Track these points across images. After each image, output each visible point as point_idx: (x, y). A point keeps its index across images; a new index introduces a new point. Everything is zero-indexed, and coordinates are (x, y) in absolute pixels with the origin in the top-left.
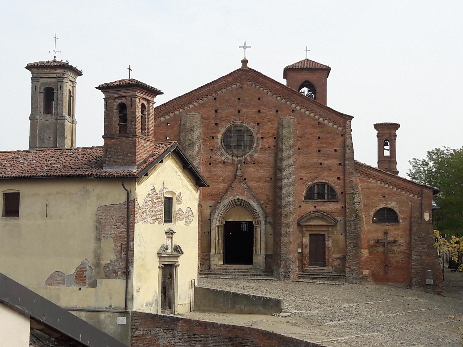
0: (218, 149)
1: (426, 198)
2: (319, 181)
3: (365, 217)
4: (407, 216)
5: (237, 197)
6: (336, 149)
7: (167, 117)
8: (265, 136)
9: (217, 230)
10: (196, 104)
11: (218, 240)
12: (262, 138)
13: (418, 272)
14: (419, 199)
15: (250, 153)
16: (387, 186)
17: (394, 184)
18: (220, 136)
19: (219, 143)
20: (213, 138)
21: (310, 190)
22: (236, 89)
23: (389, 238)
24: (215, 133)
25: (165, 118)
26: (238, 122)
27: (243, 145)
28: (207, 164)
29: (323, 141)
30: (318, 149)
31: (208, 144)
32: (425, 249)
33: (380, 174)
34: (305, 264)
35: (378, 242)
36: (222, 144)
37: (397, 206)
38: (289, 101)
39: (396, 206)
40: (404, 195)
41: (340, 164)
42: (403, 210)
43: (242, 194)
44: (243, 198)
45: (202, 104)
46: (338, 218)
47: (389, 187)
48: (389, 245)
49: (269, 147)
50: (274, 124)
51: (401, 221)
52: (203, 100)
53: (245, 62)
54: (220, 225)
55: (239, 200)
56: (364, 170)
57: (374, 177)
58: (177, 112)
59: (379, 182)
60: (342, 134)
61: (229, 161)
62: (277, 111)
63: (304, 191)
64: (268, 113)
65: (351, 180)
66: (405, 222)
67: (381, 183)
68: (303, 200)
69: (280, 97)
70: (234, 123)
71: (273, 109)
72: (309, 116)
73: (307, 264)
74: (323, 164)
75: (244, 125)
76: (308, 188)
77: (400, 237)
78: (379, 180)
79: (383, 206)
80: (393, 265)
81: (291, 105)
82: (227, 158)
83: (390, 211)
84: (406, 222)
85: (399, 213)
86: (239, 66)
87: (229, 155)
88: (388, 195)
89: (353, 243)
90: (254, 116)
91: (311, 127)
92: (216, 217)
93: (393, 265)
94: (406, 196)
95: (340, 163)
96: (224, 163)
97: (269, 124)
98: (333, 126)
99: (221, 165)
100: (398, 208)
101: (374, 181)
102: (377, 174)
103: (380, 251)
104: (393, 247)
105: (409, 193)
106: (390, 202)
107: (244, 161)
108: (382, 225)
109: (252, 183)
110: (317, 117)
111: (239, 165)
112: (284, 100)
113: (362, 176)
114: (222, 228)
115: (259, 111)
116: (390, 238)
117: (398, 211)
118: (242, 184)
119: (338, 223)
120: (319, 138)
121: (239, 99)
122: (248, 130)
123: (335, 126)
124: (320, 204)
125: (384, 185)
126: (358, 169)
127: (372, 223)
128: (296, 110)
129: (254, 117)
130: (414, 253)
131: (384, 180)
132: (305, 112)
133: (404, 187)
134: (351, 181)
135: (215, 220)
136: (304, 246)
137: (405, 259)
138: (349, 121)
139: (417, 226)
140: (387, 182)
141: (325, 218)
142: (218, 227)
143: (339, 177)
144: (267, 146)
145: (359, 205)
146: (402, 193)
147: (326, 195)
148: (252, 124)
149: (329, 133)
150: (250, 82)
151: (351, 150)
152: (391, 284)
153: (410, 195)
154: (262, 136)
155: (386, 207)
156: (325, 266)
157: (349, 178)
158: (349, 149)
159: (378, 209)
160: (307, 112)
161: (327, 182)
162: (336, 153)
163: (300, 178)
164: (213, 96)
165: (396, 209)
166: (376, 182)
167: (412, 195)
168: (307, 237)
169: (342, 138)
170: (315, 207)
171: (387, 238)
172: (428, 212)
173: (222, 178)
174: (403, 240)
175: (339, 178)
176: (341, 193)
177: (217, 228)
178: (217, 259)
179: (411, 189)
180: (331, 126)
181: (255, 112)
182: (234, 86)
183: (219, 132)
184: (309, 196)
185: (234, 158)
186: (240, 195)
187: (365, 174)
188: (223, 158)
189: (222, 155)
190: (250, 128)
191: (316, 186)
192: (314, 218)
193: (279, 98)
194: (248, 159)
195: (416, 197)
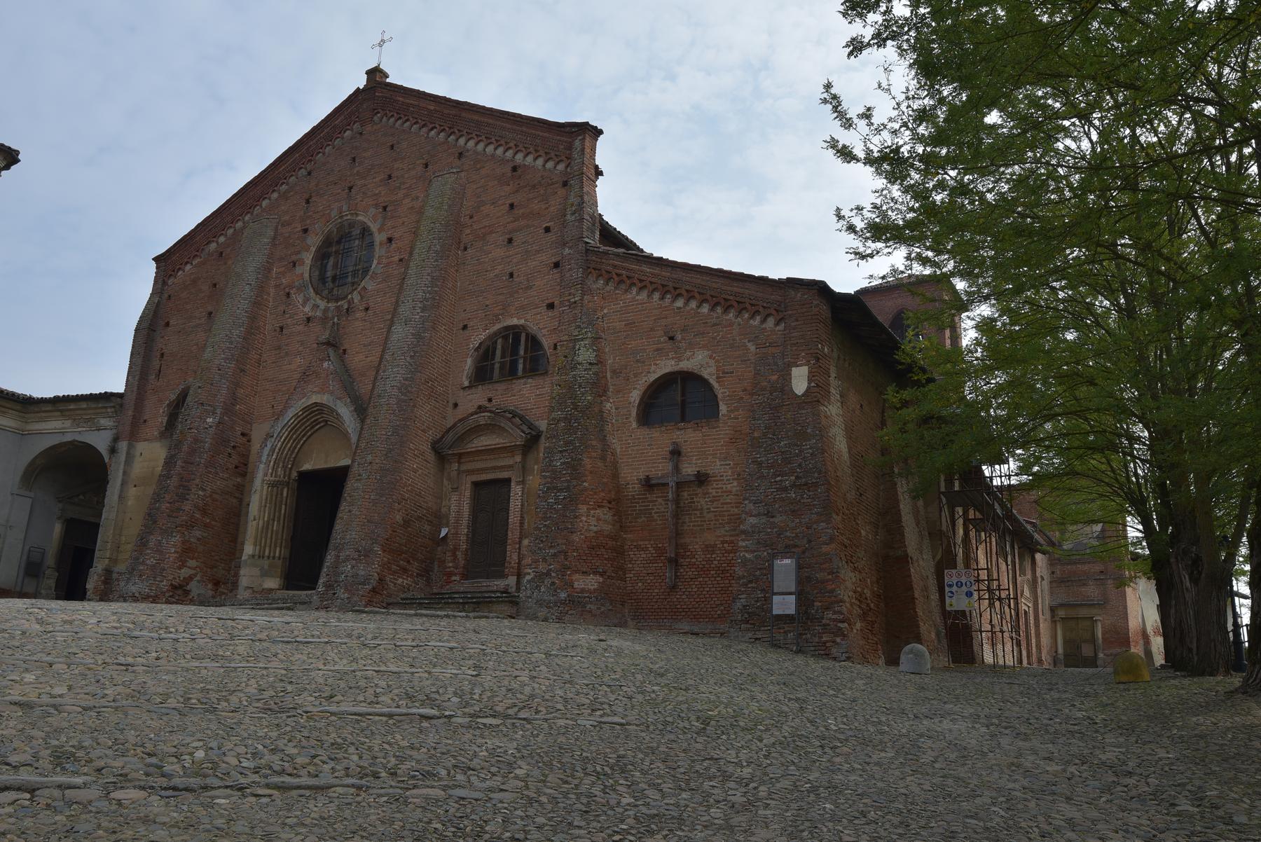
0: (301, 289)
1: (797, 320)
2: (505, 324)
3: (616, 409)
4: (745, 390)
5: (315, 398)
6: (547, 225)
7: (222, 239)
8: (396, 235)
9: (265, 493)
10: (275, 195)
11: (266, 519)
12: (390, 240)
13: (758, 573)
14: (778, 328)
15: (363, 284)
16: (680, 303)
17: (699, 293)
18: (308, 258)
19: (306, 275)
20: (294, 265)
21: (485, 354)
22: (351, 139)
23: (684, 470)
24: (299, 252)
25: (217, 242)
26: (346, 215)
27: (351, 269)
28: (275, 330)
29: (521, 211)
30: (507, 236)
31: (284, 281)
32: (785, 489)
33: (657, 271)
34: (450, 574)
35: (649, 484)
36: (310, 276)
37: (712, 362)
38: (454, 132)
39: (707, 363)
40: (731, 325)
41: (557, 265)
42: (733, 373)
43: (322, 391)
44: (324, 399)
45: (285, 193)
46: (543, 425)
47: (686, 304)
48: (685, 494)
49: (401, 260)
50: (417, 198)
51: (723, 408)
52: (287, 184)
53: (375, 74)
54: (277, 479)
55: (318, 409)
56: (615, 266)
57: (641, 281)
58: (240, 224)
59: (656, 296)
60: (565, 179)
61: (319, 314)
62: (426, 166)
63: (469, 361)
64: (406, 176)
65: (573, 300)
66: (737, 409)
67: (662, 298)
68: (466, 383)
69: (435, 130)
70: (339, 220)
71: (418, 162)
72: (493, 156)
73: (455, 575)
74: (515, 275)
75: (360, 218)
76: (481, 351)
77: (718, 463)
78: (654, 290)
79: (667, 366)
80: (694, 560)
81: (457, 140)
82: (316, 306)
83: (688, 379)
84: (741, 412)
85: (715, 385)
86: (361, 82)
87: (322, 298)
88: (684, 330)
89: (555, 488)
90: (377, 192)
91: (496, 182)
92: (264, 459)
93: (694, 560)
94: (739, 325)
95: (557, 260)
96: (309, 319)
97: (407, 201)
98: (544, 166)
99: (300, 328)
100: (713, 370)
101: (643, 295)
102: (650, 273)
103: (656, 516)
104: (698, 499)
105: (746, 316)
106: (689, 353)
107: (346, 307)
108: (663, 428)
109: (359, 358)
110: (509, 154)
111: (336, 320)
112: (442, 134)
113: (611, 287)
114: (285, 490)
115: (390, 177)
116: (689, 469)
117: (714, 377)
118: (325, 365)
119: (543, 439)
120: (512, 206)
121: (354, 159)
122: (365, 231)
123: (550, 165)
124: (501, 387)
125: (673, 302)
126: (599, 266)
127: (634, 425)
128: (468, 151)
129: (376, 195)
130: (751, 506)
131: (671, 284)
132: (484, 150)
133: (731, 298)
134: (575, 302)
135: (262, 466)
136: (452, 521)
137: (733, 538)
138: (580, 138)
139: (766, 417)
140: (678, 292)
141: (502, 425)
142: (273, 485)
143: (550, 301)
144: (396, 259)
145: (590, 369)
146: (726, 320)
147: (521, 361)
148: (372, 211)
149: (534, 187)
150: (379, 115)
151: (577, 215)
152: (685, 626)
153: (751, 322)
154: (389, 236)
155: (676, 369)
156: (503, 576)
157: (570, 294)
158: (573, 214)
159: (652, 379)
160: (490, 149)
161: (522, 322)
162: (551, 237)
163: (461, 325)
164: (306, 169)
165: (708, 373)
166: (648, 296)
167: (758, 318)
168: (468, 493)
169: (561, 192)
170: (490, 400)
171: (677, 469)
172: (801, 365)
173: (298, 359)
174: (730, 473)
175: (551, 306)
176: (552, 347)
177: (266, 487)
178: (256, 571)
179: (754, 302)
180: (540, 168)
181: (381, 181)
182: (348, 133)
183: (307, 250)
184: (482, 375)
185: (330, 305)
186: (319, 393)
187: (617, 279)
188: (307, 309)
189: (306, 300)
190: (369, 224)
191: (500, 341)
192: (478, 430)
193: (433, 133)
194: (355, 301)
195: (771, 322)
